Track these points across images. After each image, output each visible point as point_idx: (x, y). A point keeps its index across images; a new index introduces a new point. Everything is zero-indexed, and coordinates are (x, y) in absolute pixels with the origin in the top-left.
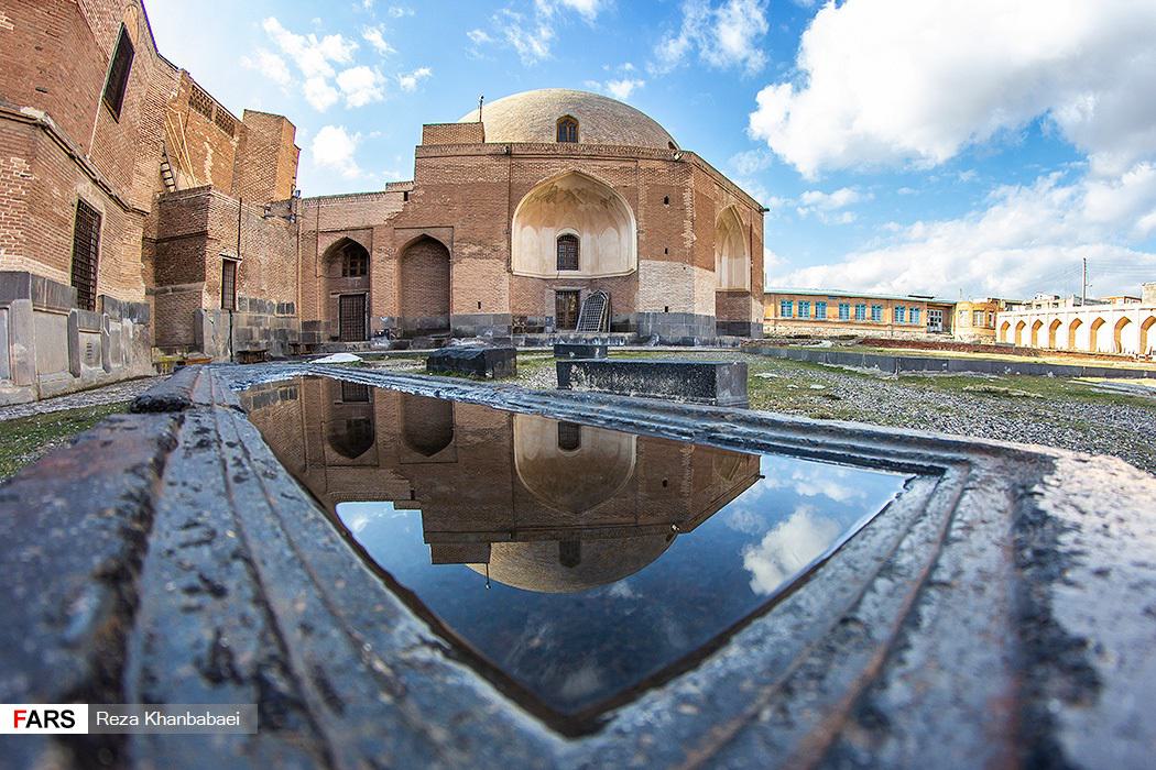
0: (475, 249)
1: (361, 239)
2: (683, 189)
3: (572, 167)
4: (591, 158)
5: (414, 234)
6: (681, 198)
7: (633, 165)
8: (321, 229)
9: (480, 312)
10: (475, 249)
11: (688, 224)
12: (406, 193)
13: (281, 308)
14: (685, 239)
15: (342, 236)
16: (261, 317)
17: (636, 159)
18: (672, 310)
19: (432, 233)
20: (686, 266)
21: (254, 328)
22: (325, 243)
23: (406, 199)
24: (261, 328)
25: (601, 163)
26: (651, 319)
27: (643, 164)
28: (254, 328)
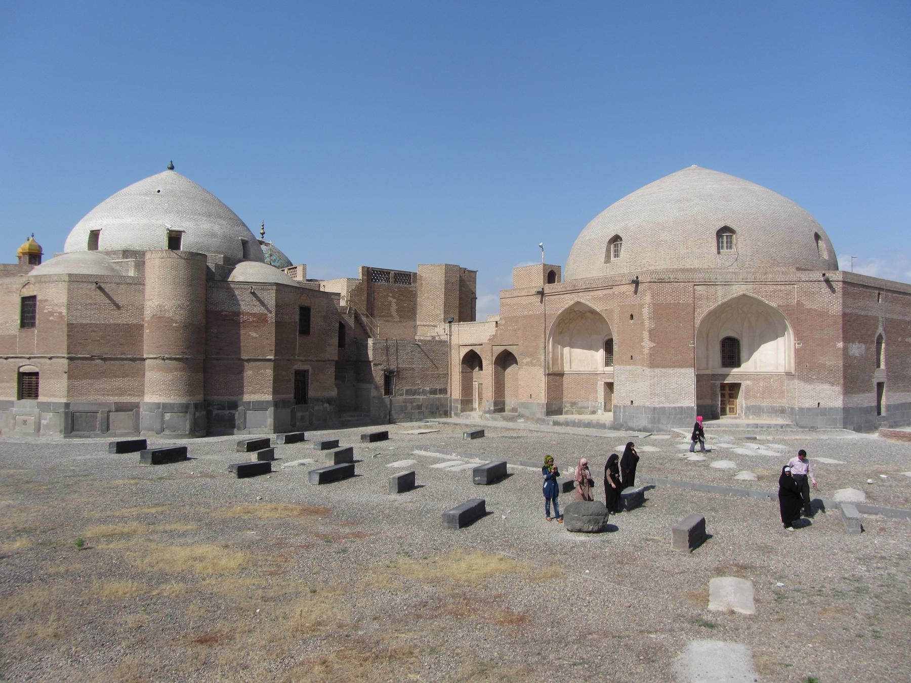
0: (528, 360)
1: (477, 350)
2: (641, 306)
3: (576, 299)
4: (587, 290)
5: (501, 349)
6: (641, 314)
7: (609, 291)
8: (461, 343)
9: (530, 401)
10: (528, 360)
11: (646, 334)
12: (497, 322)
13: (433, 392)
14: (643, 347)
15: (470, 348)
16: (415, 398)
17: (611, 287)
18: (636, 404)
19: (510, 349)
20: (644, 368)
21: (408, 404)
22: (464, 351)
23: (497, 327)
24: (414, 404)
25: (592, 293)
26: (622, 410)
27: (616, 290)
28: (408, 404)
